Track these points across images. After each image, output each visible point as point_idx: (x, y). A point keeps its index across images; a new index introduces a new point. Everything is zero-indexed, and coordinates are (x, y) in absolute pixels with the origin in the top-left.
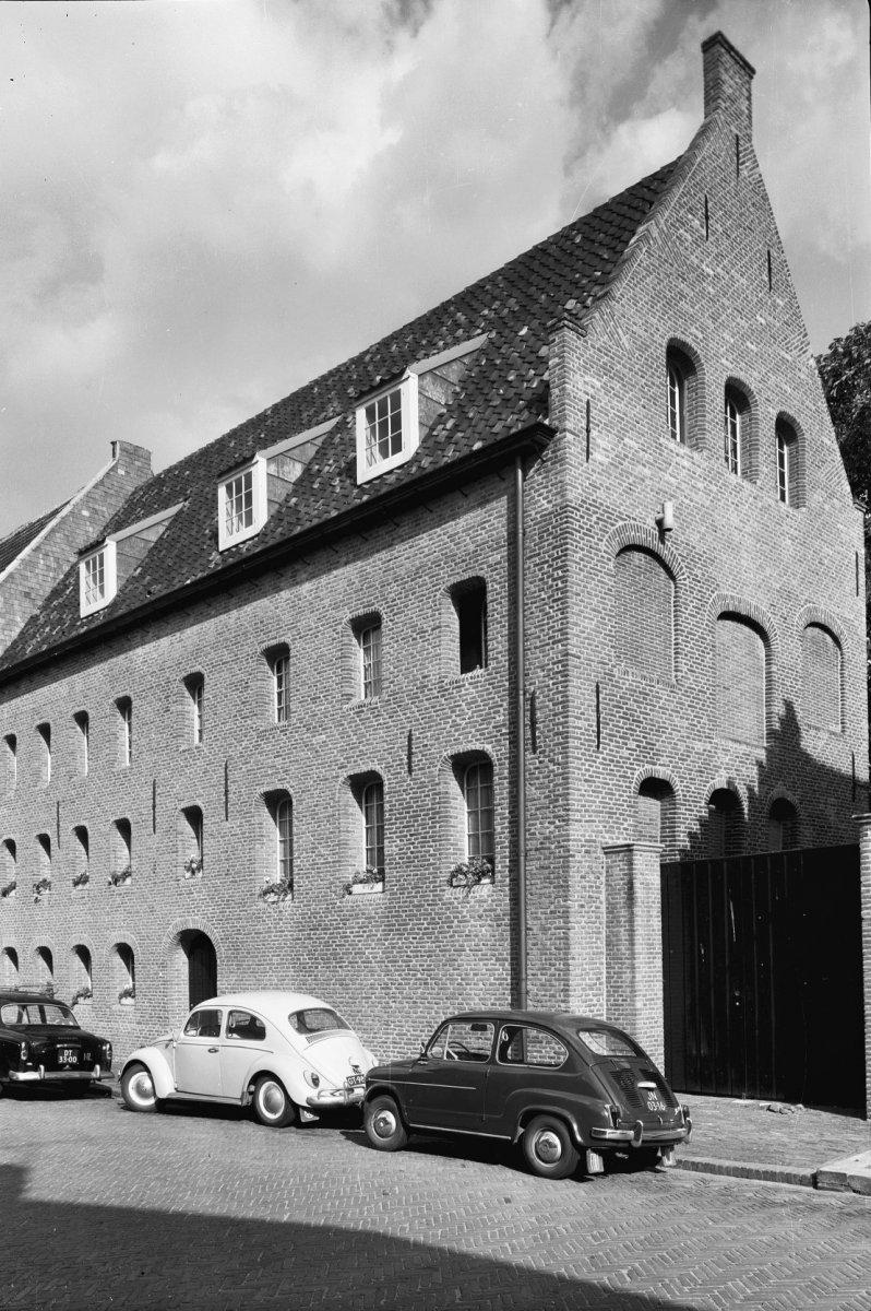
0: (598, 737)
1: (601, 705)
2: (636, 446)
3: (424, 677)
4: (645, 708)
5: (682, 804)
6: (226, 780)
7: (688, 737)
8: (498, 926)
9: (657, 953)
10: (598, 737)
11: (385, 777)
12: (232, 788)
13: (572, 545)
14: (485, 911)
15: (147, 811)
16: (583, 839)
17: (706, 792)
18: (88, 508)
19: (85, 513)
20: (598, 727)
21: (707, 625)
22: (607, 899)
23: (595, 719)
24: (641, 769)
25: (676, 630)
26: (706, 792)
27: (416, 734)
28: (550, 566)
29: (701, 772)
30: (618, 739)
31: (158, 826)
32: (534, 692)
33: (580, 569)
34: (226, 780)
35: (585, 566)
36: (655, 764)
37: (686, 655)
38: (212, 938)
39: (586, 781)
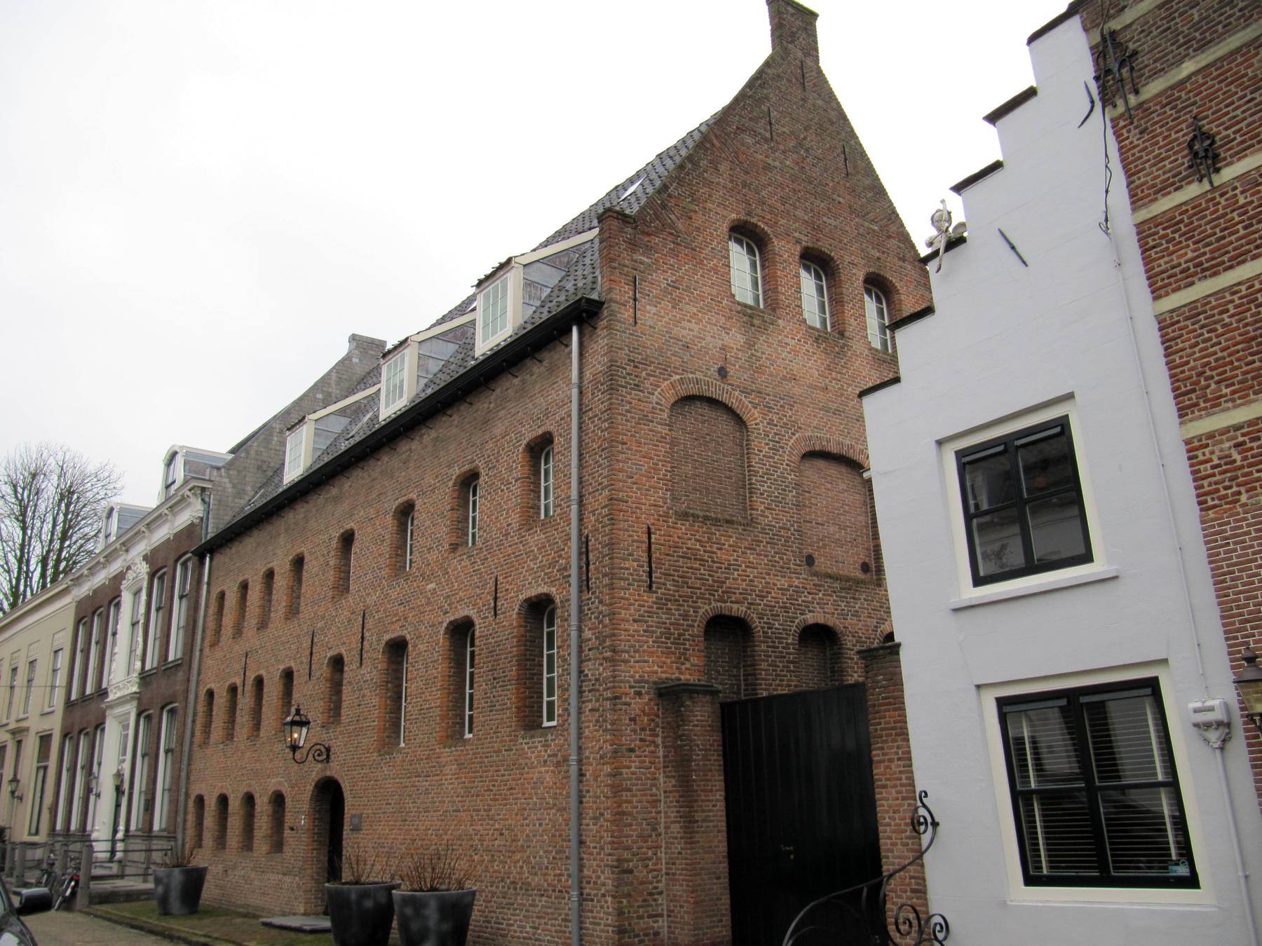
0: (650, 577)
1: (653, 546)
2: (695, 310)
3: (508, 525)
4: (711, 547)
5: (761, 642)
6: (363, 628)
7: (769, 574)
8: (559, 773)
9: (717, 800)
10: (650, 577)
11: (477, 621)
12: (367, 634)
13: (617, 399)
14: (549, 756)
15: (356, 653)
16: (631, 680)
17: (794, 628)
18: (323, 392)
19: (320, 396)
20: (650, 567)
21: (787, 465)
22: (663, 742)
23: (647, 560)
24: (707, 607)
25: (749, 471)
26: (794, 628)
27: (500, 578)
28: (600, 419)
29: (786, 607)
30: (676, 578)
31: (313, 674)
32: (587, 536)
33: (627, 421)
34: (363, 628)
35: (632, 417)
36: (725, 602)
37: (761, 494)
38: (343, 785)
39: (635, 621)
